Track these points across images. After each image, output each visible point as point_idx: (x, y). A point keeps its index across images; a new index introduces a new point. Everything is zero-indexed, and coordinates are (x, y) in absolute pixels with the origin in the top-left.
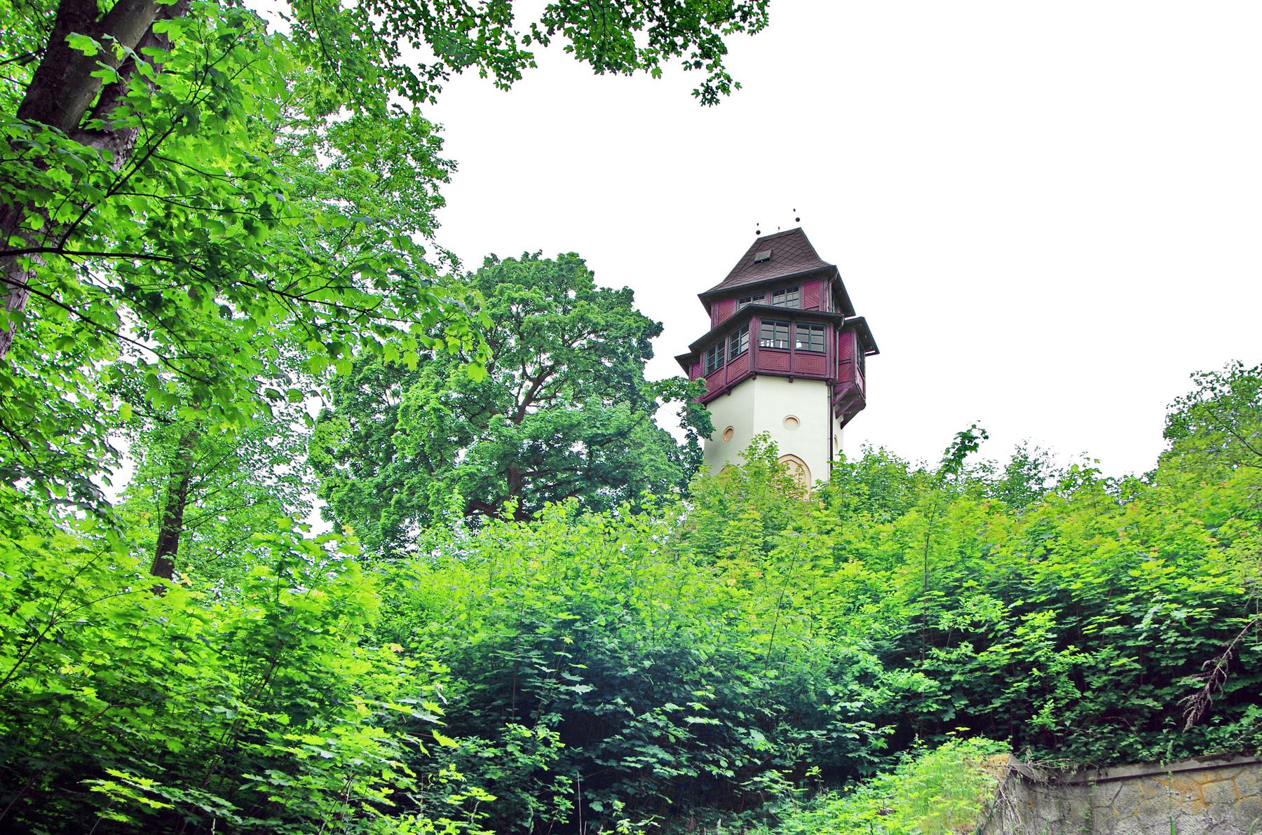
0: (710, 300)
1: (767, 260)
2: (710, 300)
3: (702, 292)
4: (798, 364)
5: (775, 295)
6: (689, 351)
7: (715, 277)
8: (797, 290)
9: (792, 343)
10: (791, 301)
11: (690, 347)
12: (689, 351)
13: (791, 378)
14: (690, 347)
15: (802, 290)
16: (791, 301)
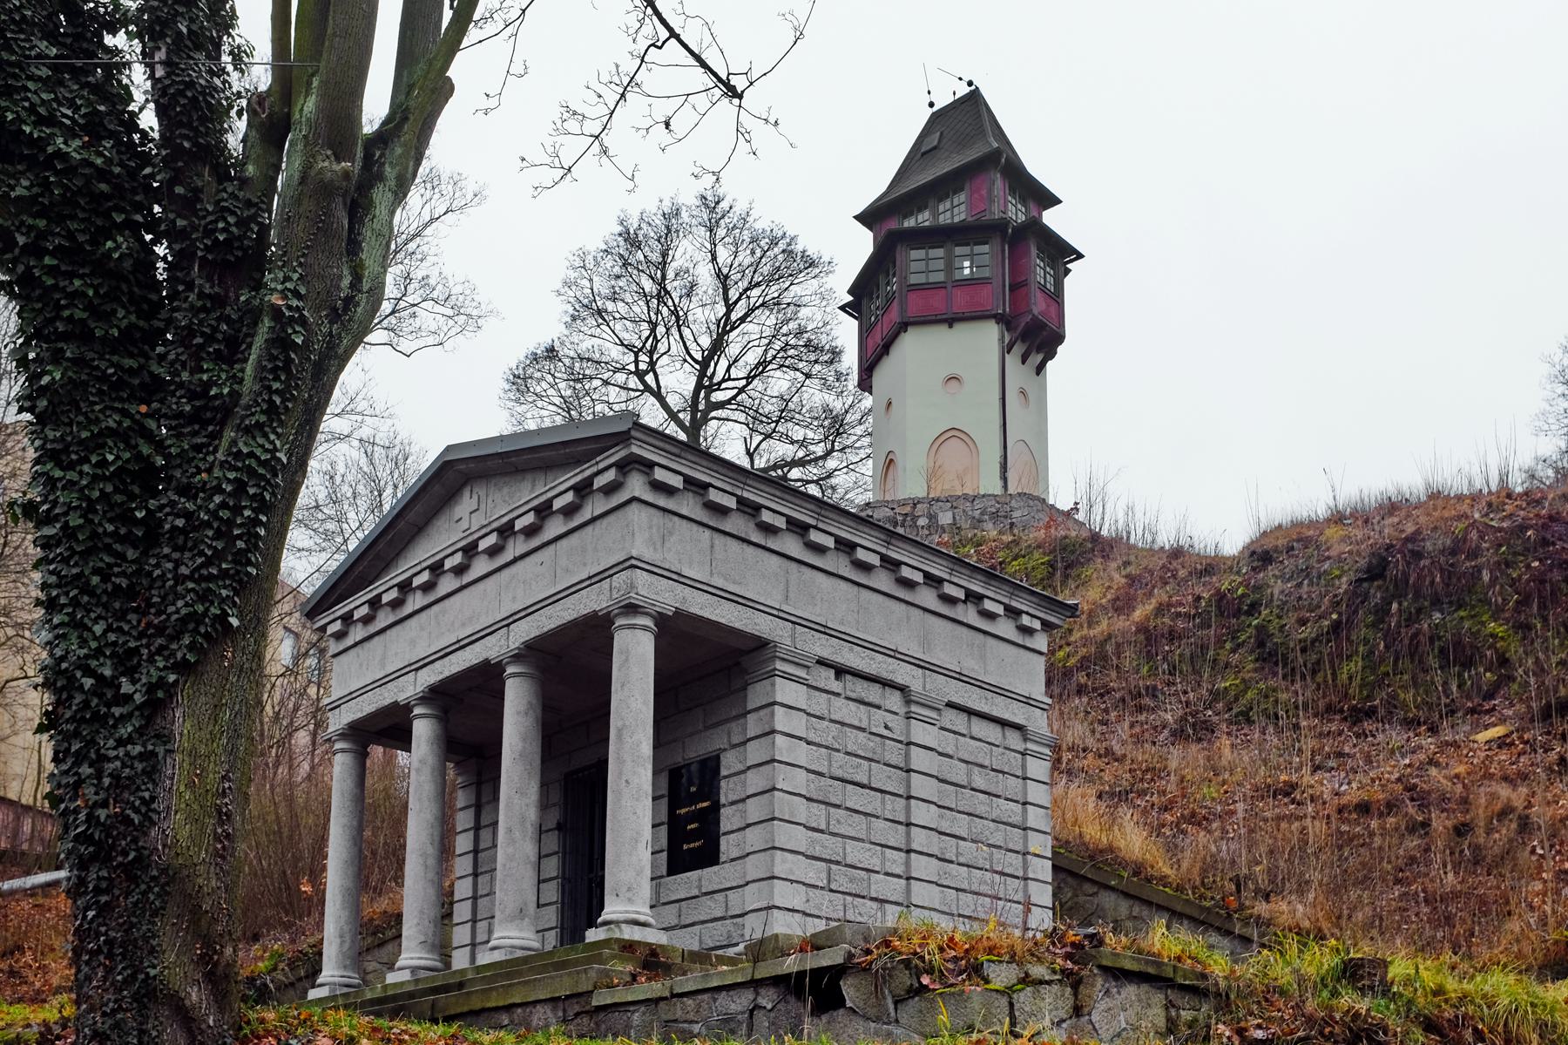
0: (867, 218)
1: (935, 148)
2: (867, 218)
3: (861, 206)
4: (960, 301)
5: (941, 200)
6: (850, 298)
7: (874, 184)
8: (962, 190)
9: (950, 267)
10: (954, 211)
11: (850, 292)
12: (850, 298)
13: (951, 322)
14: (850, 292)
15: (967, 186)
16: (954, 211)
